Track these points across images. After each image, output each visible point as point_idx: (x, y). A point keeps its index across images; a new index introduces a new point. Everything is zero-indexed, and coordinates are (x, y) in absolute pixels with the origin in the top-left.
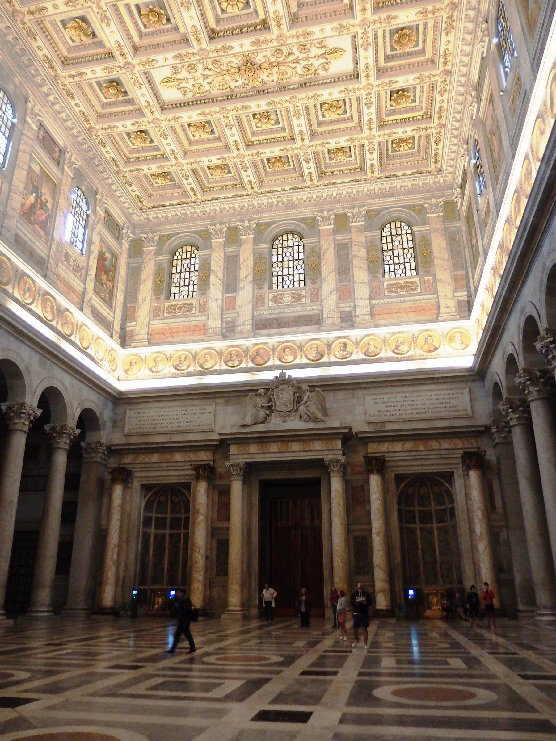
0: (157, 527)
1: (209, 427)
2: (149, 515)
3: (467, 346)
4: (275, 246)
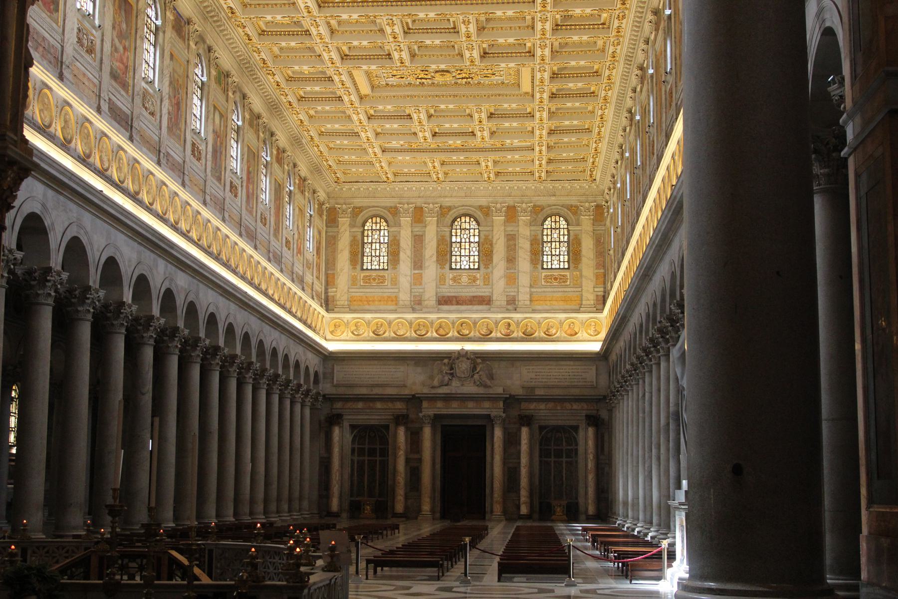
0: (359, 455)
1: (402, 383)
2: (354, 446)
3: (599, 333)
4: (454, 227)
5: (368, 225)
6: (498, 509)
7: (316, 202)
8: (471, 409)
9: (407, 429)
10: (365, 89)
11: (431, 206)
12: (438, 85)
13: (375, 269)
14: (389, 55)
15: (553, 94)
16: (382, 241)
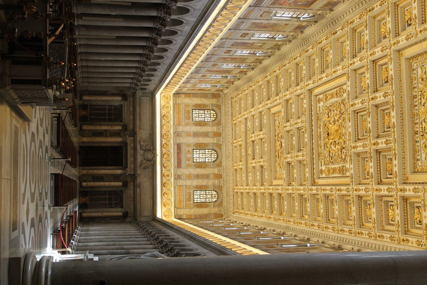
3: (165, 217)
5: (212, 112)
6: (85, 172)
7: (223, 89)
8: (130, 159)
9: (121, 130)
10: (273, 110)
11: (222, 140)
12: (275, 143)
13: (193, 115)
14: (288, 121)
15: (272, 194)
16: (205, 118)
